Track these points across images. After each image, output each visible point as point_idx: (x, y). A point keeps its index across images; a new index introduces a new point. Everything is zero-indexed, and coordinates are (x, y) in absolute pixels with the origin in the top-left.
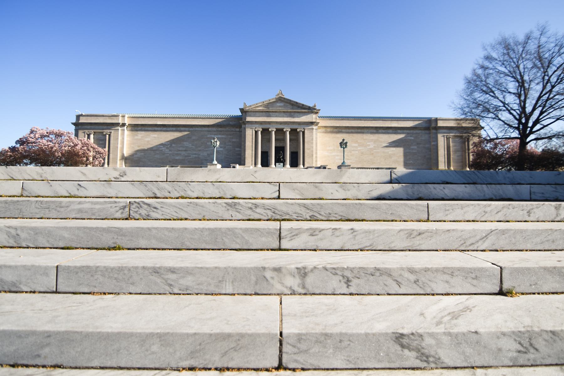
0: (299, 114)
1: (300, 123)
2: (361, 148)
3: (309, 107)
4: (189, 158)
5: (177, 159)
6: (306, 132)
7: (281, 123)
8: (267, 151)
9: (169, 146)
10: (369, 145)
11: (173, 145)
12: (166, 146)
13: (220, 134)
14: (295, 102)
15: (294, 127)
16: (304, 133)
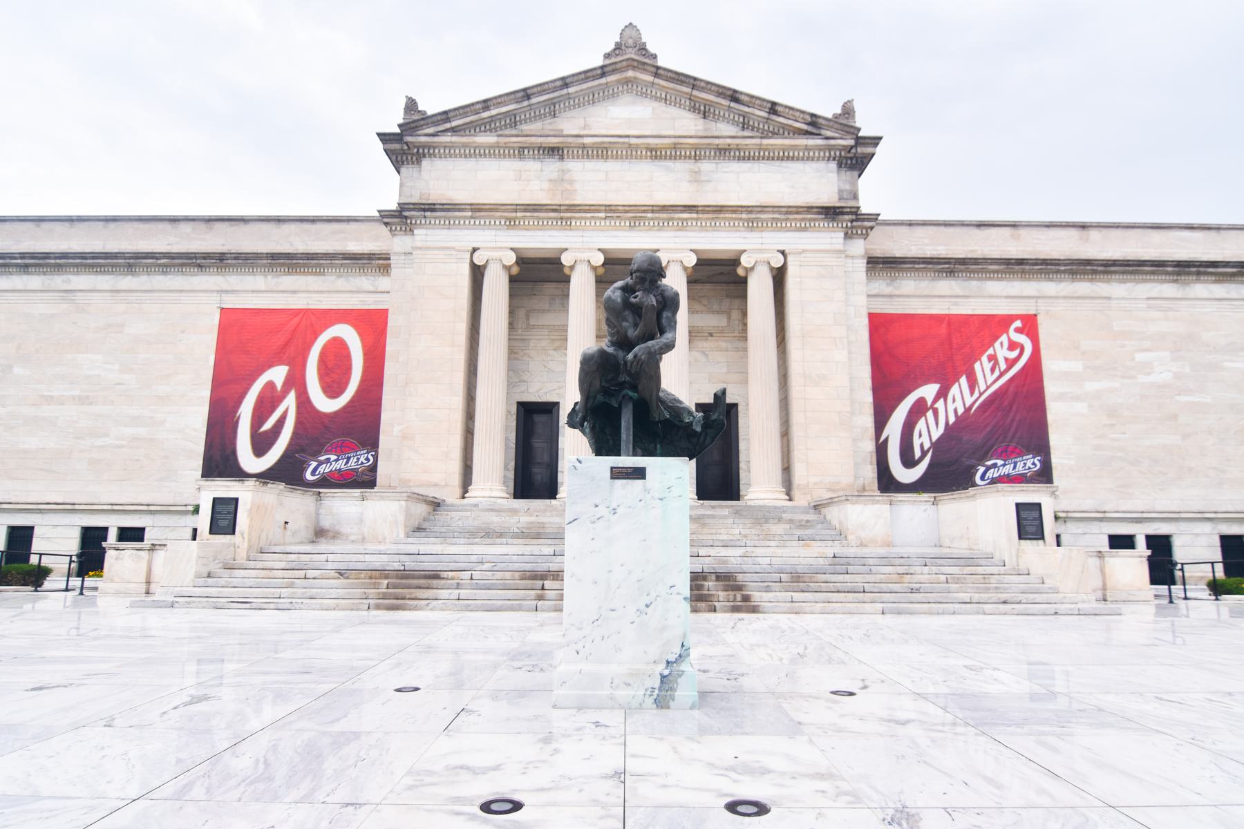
4: (99, 442)
7: (636, 215)
8: (554, 400)
11: (17, 370)
16: (779, 277)
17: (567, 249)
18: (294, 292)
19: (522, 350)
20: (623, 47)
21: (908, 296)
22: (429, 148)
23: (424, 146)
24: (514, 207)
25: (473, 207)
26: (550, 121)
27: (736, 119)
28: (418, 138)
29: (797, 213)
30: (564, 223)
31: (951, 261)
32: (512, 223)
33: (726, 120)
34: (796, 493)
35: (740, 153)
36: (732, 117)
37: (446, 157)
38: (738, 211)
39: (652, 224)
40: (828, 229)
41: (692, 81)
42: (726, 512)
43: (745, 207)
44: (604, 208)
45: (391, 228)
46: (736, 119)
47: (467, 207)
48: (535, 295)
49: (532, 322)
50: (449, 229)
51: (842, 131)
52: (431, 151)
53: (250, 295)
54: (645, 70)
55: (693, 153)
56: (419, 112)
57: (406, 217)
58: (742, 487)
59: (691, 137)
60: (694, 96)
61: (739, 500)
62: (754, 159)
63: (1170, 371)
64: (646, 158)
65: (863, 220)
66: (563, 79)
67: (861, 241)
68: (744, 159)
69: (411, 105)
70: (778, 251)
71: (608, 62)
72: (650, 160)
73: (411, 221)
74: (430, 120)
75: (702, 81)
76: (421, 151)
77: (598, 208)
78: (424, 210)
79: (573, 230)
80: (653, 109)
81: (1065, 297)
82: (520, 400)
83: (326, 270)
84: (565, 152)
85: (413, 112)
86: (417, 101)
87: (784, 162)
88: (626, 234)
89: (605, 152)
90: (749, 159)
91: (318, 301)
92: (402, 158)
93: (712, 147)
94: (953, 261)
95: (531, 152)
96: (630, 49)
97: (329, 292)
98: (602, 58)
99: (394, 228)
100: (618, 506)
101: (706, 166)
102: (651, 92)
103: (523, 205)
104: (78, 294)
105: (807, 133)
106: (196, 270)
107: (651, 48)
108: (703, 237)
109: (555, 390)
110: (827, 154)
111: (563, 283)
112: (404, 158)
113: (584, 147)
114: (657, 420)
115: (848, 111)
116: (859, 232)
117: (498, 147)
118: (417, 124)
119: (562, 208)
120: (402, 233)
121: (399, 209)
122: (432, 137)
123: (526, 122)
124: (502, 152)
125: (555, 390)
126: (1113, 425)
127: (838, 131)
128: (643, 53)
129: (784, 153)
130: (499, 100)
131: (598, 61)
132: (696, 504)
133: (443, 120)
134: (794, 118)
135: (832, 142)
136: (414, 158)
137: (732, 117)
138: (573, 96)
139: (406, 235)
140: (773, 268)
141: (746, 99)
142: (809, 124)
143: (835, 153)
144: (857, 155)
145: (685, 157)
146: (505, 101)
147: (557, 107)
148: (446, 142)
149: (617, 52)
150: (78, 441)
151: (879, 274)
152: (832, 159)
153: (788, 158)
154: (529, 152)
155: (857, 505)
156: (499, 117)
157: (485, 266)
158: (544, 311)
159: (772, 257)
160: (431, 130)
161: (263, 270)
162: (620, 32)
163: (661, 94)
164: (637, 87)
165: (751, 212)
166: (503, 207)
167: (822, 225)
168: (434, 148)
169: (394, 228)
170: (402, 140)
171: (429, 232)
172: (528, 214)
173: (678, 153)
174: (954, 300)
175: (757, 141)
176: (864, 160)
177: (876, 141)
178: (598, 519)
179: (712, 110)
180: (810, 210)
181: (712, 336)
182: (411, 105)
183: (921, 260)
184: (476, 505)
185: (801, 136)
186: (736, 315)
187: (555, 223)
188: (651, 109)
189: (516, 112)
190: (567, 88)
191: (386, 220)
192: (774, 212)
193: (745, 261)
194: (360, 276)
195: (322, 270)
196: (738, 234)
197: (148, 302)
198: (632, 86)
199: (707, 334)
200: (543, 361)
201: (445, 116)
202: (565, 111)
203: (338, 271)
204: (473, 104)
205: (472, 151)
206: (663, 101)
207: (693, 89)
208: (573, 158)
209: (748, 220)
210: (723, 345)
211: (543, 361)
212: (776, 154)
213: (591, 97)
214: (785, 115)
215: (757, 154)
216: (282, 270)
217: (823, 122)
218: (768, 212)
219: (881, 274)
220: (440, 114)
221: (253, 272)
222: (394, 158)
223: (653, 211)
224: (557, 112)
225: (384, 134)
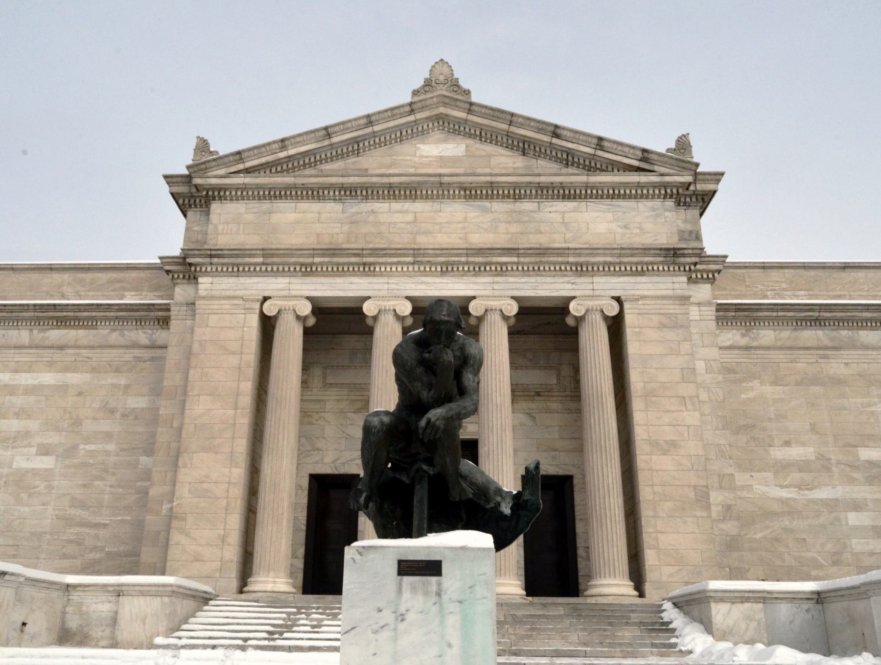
0: (570, 205)
3: (645, 155)
6: (629, 319)
13: (51, 365)
14: (541, 126)
17: (369, 298)
18: (61, 348)
19: (317, 412)
20: (433, 84)
21: (768, 348)
22: (219, 190)
24: (311, 252)
25: (265, 252)
26: (353, 160)
27: (559, 155)
28: (208, 179)
29: (632, 255)
30: (367, 269)
31: (815, 307)
32: (309, 269)
33: (548, 157)
34: (648, 588)
35: (564, 191)
36: (554, 154)
37: (238, 200)
38: (565, 254)
39: (466, 268)
40: (668, 273)
41: (508, 117)
42: (561, 611)
43: (572, 249)
44: (411, 252)
45: (173, 276)
46: (559, 155)
47: (258, 252)
48: (333, 349)
50: (238, 276)
51: (678, 167)
52: (222, 194)
53: (13, 351)
54: (457, 106)
55: (512, 192)
57: (190, 264)
58: (581, 580)
59: (509, 175)
60: (512, 133)
61: (578, 596)
62: (580, 198)
64: (459, 198)
65: (708, 263)
66: (368, 116)
67: (708, 287)
68: (569, 198)
69: (203, 146)
70: (613, 298)
71: (416, 99)
72: (464, 200)
73: (196, 269)
74: (219, 162)
76: (210, 193)
77: (406, 252)
78: (211, 256)
79: (378, 276)
82: (313, 472)
83: (99, 323)
84: (370, 192)
85: (203, 154)
86: (209, 142)
87: (613, 200)
88: (437, 280)
89: (413, 192)
90: (575, 198)
91: (88, 358)
92: (189, 201)
93: (532, 185)
94: (818, 307)
97: (100, 347)
98: (410, 95)
99: (176, 276)
100: (407, 611)
101: (527, 206)
102: (465, 128)
103: (321, 249)
105: (639, 169)
107: (464, 84)
108: (526, 283)
110: (663, 192)
111: (366, 336)
112: (192, 201)
113: (390, 187)
114: (457, 500)
115: (683, 144)
116: (705, 276)
117: (296, 188)
118: (208, 165)
119: (365, 252)
121: (183, 256)
122: (223, 179)
123: (326, 162)
124: (299, 193)
127: (673, 167)
128: (455, 89)
129: (614, 191)
130: (298, 139)
131: (407, 98)
132: (525, 601)
133: (236, 161)
134: (623, 154)
135: (667, 179)
136: (203, 201)
137: (554, 154)
138: (379, 134)
140: (608, 316)
141: (569, 134)
143: (672, 191)
144: (696, 193)
145: (504, 197)
146: (304, 141)
147: (361, 145)
148: (239, 184)
149: (427, 89)
151: (732, 323)
152: (668, 196)
153: (619, 196)
155: (721, 603)
156: (297, 157)
157: (276, 318)
158: (343, 367)
159: (606, 304)
160: (222, 172)
161: (28, 324)
162: (430, 69)
163: (475, 131)
164: (449, 124)
165: (580, 255)
166: (298, 252)
167: (661, 268)
168: (225, 190)
169: (176, 276)
170: (190, 182)
171: (216, 280)
172: (326, 259)
173: (495, 192)
174: (822, 352)
175: (584, 179)
176: (705, 197)
177: (718, 177)
178: (382, 627)
179: (532, 147)
180: (647, 252)
181: (539, 395)
182: (203, 146)
183: (780, 307)
185: (632, 173)
186: (566, 371)
187: (356, 269)
189: (315, 151)
190: (372, 126)
191: (167, 268)
192: (605, 255)
193: (575, 308)
194: (137, 329)
195: (94, 323)
196: (566, 279)
198: (444, 123)
201: (239, 155)
202: (370, 150)
203: (112, 323)
204: (269, 144)
205: (267, 193)
206: (478, 138)
207: (510, 125)
208: (378, 199)
209: (576, 264)
211: (341, 425)
212: (606, 192)
213: (398, 134)
214: (613, 151)
215: (583, 192)
216: (50, 323)
217: (656, 157)
218: (599, 254)
219: (734, 324)
220: (232, 154)
221: (17, 325)
222: (181, 201)
223: (467, 255)
224: (361, 151)
225: (171, 176)
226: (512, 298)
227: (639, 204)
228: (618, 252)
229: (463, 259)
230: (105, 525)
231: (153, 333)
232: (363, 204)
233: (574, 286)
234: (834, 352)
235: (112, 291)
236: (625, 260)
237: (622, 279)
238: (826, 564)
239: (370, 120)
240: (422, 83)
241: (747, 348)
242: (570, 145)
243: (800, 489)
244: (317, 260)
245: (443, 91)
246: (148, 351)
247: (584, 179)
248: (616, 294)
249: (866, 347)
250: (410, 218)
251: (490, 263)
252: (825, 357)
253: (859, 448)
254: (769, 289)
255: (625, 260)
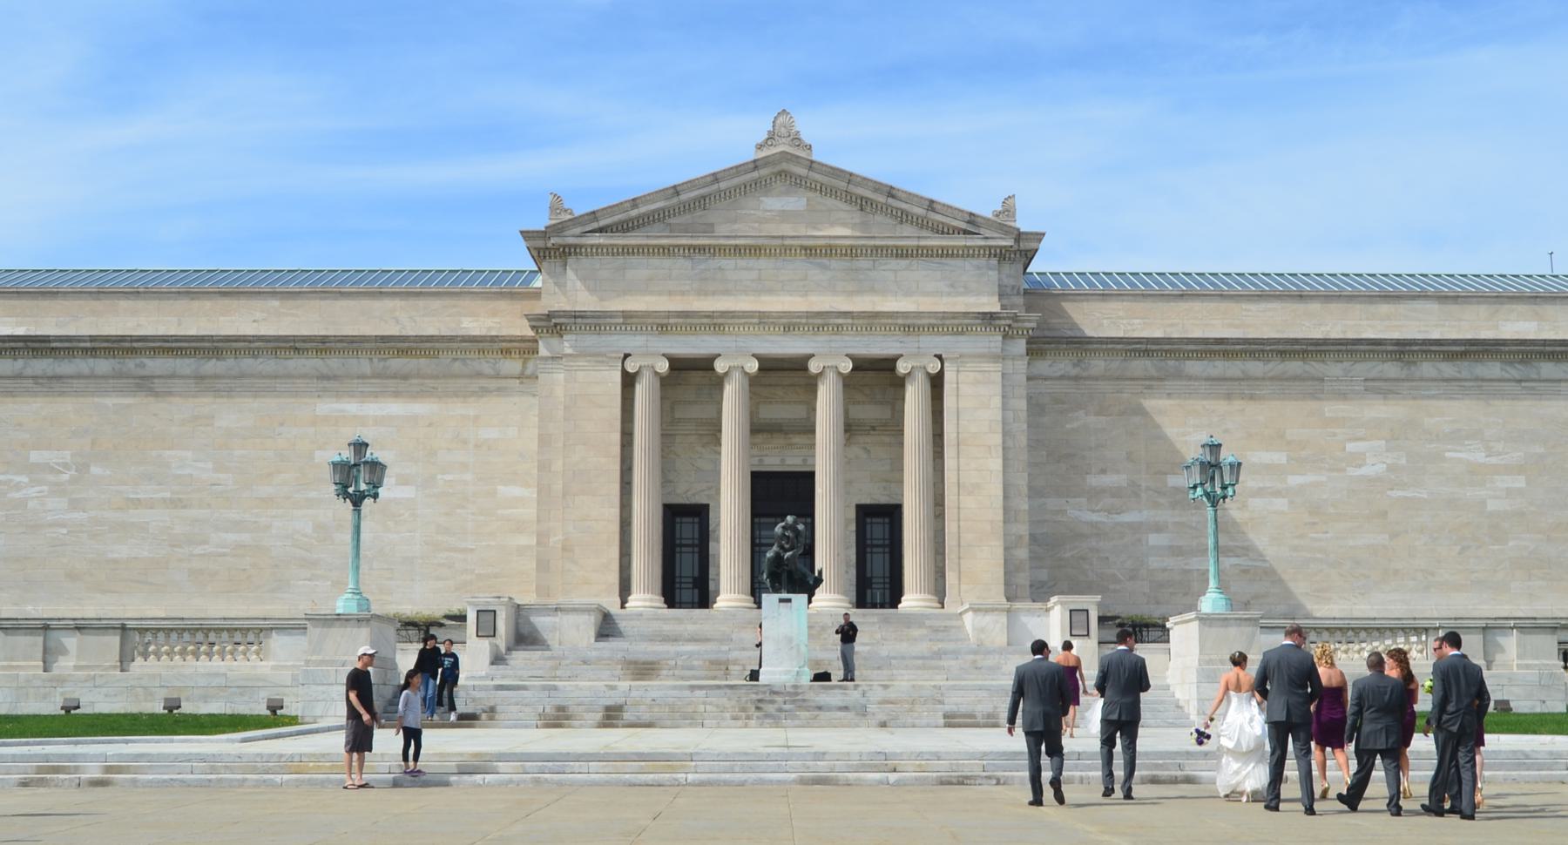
0: (904, 263)
1: (909, 325)
2: (1310, 478)
3: (972, 219)
4: (198, 550)
5: (115, 561)
6: (949, 376)
7: (790, 324)
8: (704, 501)
9: (66, 477)
10: (1358, 460)
11: (95, 470)
12: (51, 478)
14: (877, 187)
15: (876, 346)
18: (405, 377)
20: (776, 137)
23: (570, 246)
41: (848, 176)
48: (680, 384)
49: (678, 415)
52: (578, 250)
53: (356, 381)
54: (798, 163)
56: (566, 211)
63: (1384, 463)
66: (714, 174)
68: (902, 256)
70: (936, 356)
71: (761, 154)
75: (857, 176)
76: (567, 250)
78: (575, 317)
80: (808, 200)
81: (1272, 379)
82: (668, 502)
85: (558, 211)
91: (433, 388)
95: (681, 251)
96: (784, 140)
97: (445, 377)
101: (863, 263)
104: (156, 381)
105: (966, 232)
106: (292, 353)
107: (806, 137)
108: (859, 341)
109: (703, 491)
115: (1008, 209)
120: (548, 335)
125: (703, 491)
126: (1314, 524)
131: (750, 155)
139: (552, 337)
141: (904, 195)
142: (968, 222)
143: (995, 251)
150: (176, 549)
154: (679, 250)
160: (578, 230)
174: (1147, 383)
176: (1028, 253)
181: (874, 430)
184: (641, 615)
188: (805, 199)
192: (930, 317)
197: (238, 390)
199: (868, 428)
200: (691, 458)
201: (593, 215)
204: (621, 203)
208: (725, 256)
210: (887, 439)
211: (691, 458)
215: (915, 252)
225: (528, 232)
226: (847, 355)
227: (966, 263)
228: (941, 315)
229: (804, 321)
230: (472, 550)
231: (496, 363)
232: (711, 261)
233: (902, 345)
234: (1159, 383)
235: (447, 316)
236: (947, 322)
237: (946, 338)
238: (1122, 578)
239: (716, 177)
240: (766, 136)
241: (1076, 378)
242: (904, 206)
243: (1109, 513)
244: (672, 321)
245: (782, 147)
246: (494, 381)
247: (914, 243)
248: (938, 353)
249: (1190, 378)
250: (754, 274)
251: (828, 325)
252: (1149, 387)
253: (1169, 476)
254: (1106, 316)
255: (947, 322)
